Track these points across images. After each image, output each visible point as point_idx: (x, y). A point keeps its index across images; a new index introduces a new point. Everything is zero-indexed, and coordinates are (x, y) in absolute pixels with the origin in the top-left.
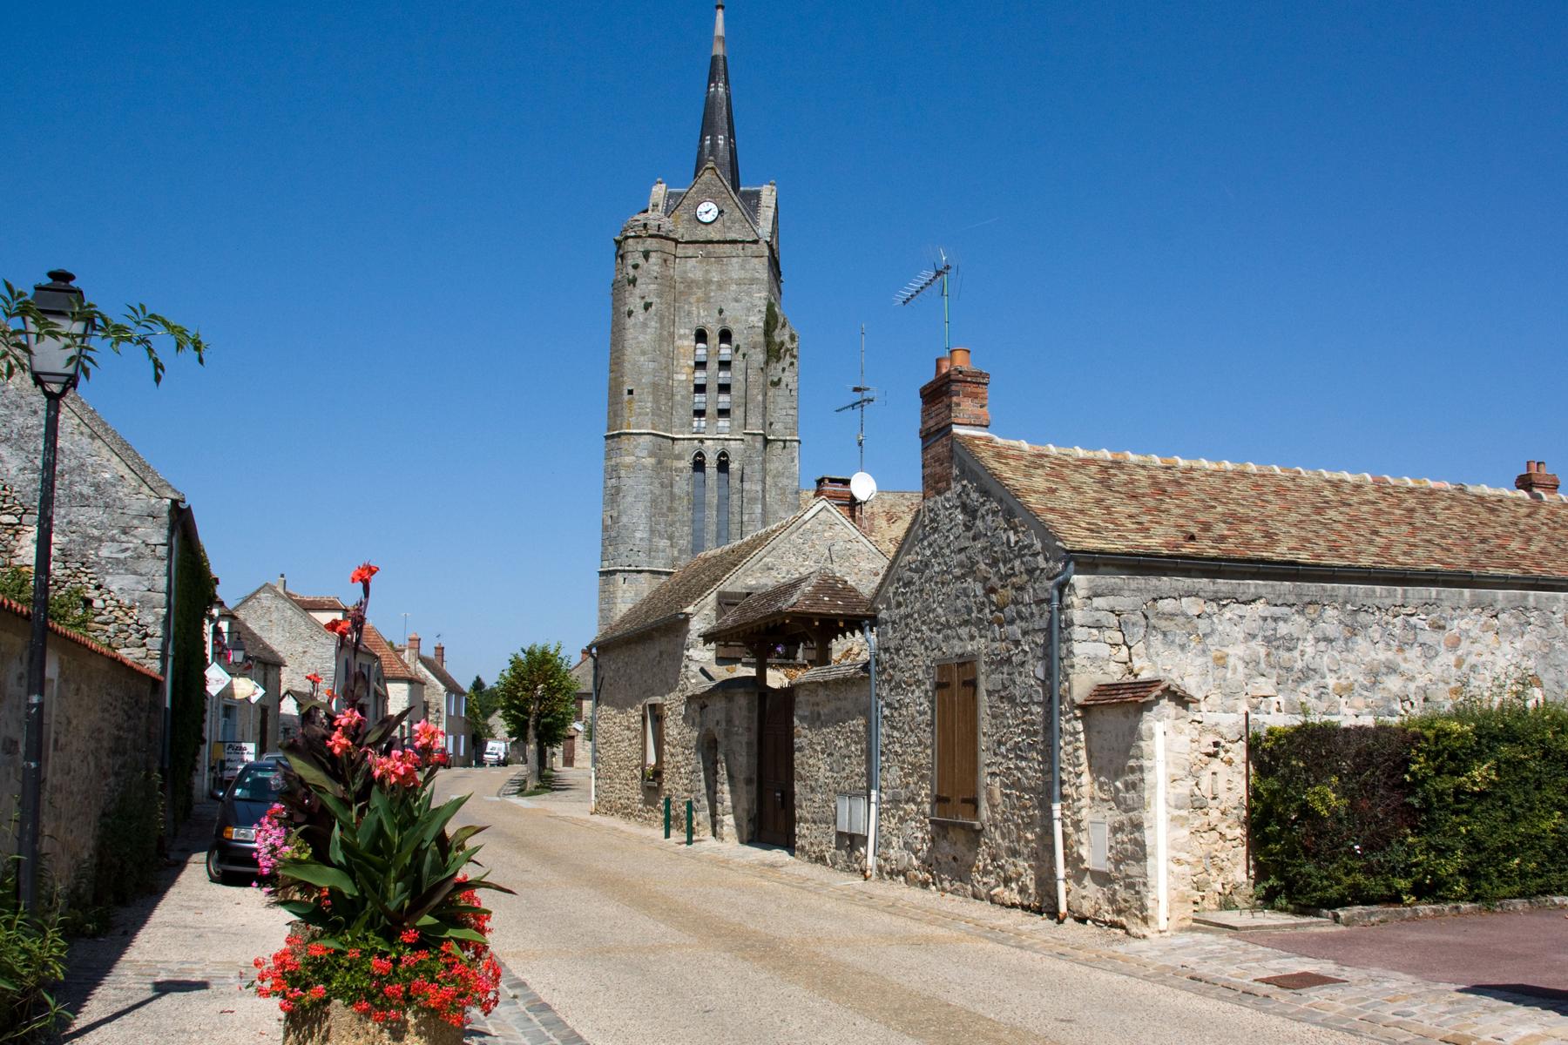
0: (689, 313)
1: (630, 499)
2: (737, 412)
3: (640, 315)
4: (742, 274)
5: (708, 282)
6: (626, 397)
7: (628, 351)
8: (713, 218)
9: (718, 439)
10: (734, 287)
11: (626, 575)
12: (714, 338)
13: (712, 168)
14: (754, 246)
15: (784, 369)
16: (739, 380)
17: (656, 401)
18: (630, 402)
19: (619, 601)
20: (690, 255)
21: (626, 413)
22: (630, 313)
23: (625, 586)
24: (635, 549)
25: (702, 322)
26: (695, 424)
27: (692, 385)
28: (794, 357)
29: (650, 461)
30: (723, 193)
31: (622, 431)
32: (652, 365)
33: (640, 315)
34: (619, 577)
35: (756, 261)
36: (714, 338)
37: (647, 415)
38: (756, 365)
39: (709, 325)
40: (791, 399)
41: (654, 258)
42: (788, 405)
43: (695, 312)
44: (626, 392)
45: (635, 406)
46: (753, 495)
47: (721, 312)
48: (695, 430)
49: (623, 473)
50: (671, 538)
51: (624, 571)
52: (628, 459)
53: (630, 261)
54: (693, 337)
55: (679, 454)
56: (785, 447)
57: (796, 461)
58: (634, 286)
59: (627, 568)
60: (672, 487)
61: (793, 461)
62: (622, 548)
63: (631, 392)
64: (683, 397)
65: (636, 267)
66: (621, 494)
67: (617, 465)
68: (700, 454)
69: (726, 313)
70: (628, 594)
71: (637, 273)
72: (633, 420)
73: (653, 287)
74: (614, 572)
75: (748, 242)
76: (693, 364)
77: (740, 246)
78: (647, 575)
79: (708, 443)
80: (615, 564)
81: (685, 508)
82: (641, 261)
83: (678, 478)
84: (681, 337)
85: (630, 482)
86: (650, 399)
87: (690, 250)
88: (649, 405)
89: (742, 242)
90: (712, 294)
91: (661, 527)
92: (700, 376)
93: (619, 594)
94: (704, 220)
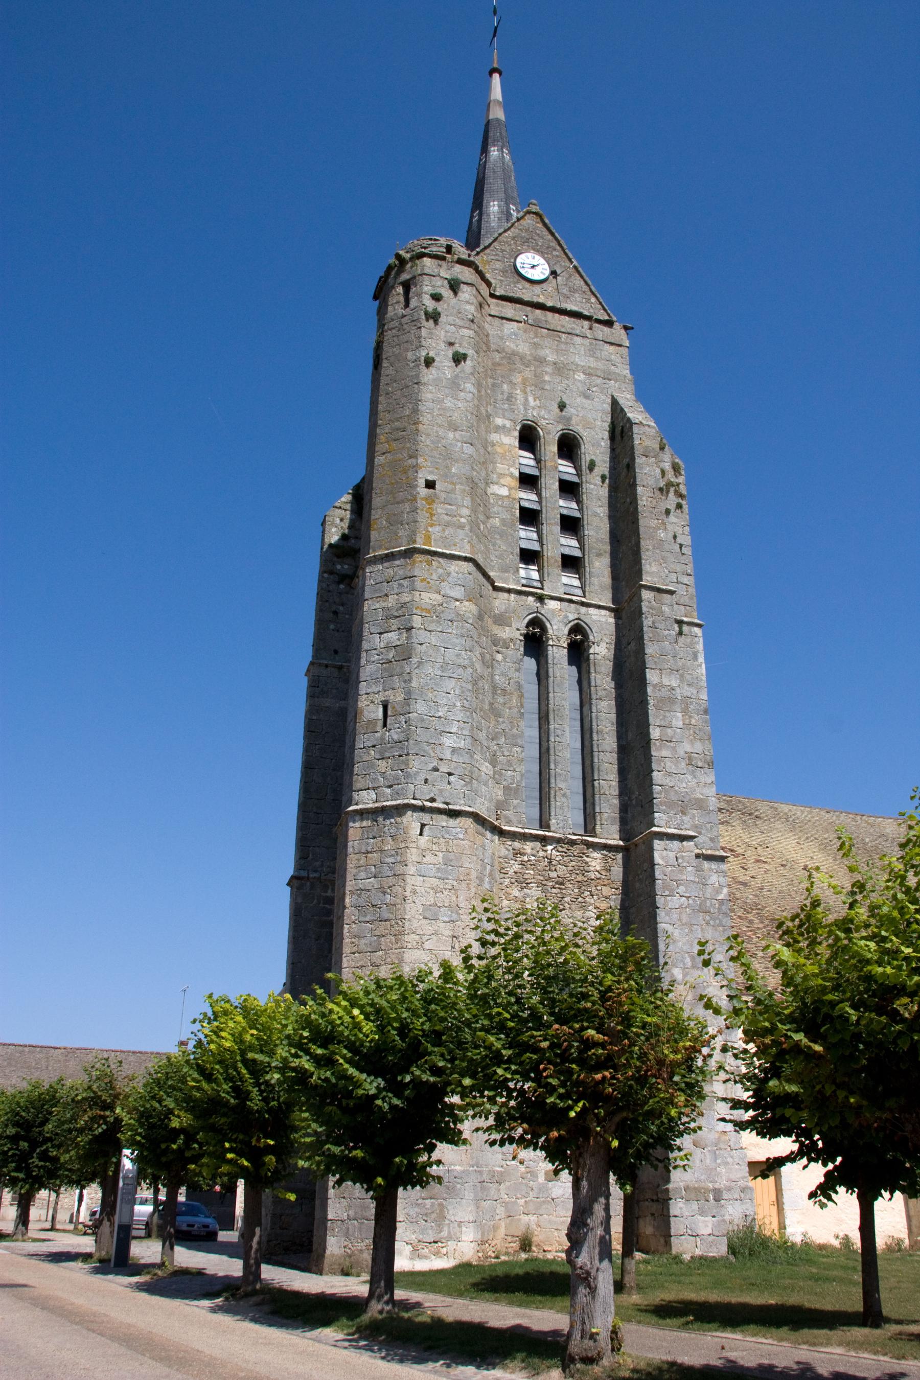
0: (510, 398)
1: (429, 669)
2: (597, 564)
3: (444, 366)
4: (592, 363)
5: (542, 361)
6: (423, 492)
7: (425, 418)
8: (542, 277)
9: (571, 601)
10: (580, 376)
11: (426, 818)
12: (550, 448)
13: (536, 214)
14: (606, 329)
15: (668, 512)
16: (596, 515)
17: (474, 511)
18: (430, 500)
19: (412, 869)
20: (509, 316)
21: (422, 517)
22: (429, 362)
23: (423, 840)
24: (444, 768)
25: (533, 414)
26: (522, 573)
27: (517, 507)
28: (681, 496)
29: (468, 608)
30: (555, 250)
31: (417, 546)
32: (469, 450)
33: (444, 366)
34: (412, 821)
35: (612, 349)
36: (550, 448)
37: (462, 527)
38: (651, 482)
39: (543, 422)
40: (683, 559)
41: (466, 293)
42: (679, 568)
43: (520, 398)
44: (422, 483)
45: (440, 509)
46: (664, 693)
47: (562, 406)
48: (524, 582)
49: (417, 621)
50: (493, 762)
51: (422, 809)
52: (428, 598)
53: (427, 289)
54: (517, 434)
55: (501, 615)
56: (680, 633)
57: (701, 659)
58: (436, 322)
59: (428, 804)
60: (492, 668)
61: (695, 658)
62: (415, 764)
63: (430, 485)
64: (503, 521)
65: (437, 298)
66: (414, 660)
67: (403, 605)
68: (536, 622)
69: (569, 411)
70: (429, 858)
71: (441, 307)
72: (435, 531)
73: (466, 332)
74: (400, 810)
75: (599, 321)
76: (517, 474)
77: (586, 324)
78: (468, 822)
79: (552, 605)
80: (398, 794)
81: (515, 710)
82: (446, 293)
83: (499, 657)
84: (497, 429)
85: (434, 639)
86: (467, 501)
87: (509, 310)
88: (465, 512)
89: (588, 318)
90: (547, 378)
91: (482, 736)
92: (528, 498)
93: (413, 855)
94: (529, 276)
